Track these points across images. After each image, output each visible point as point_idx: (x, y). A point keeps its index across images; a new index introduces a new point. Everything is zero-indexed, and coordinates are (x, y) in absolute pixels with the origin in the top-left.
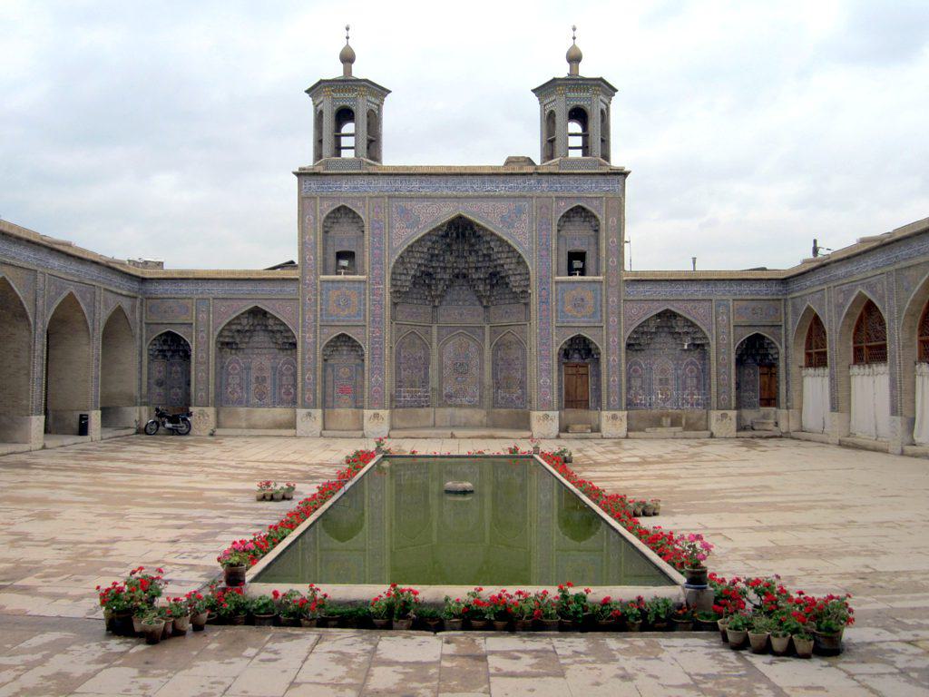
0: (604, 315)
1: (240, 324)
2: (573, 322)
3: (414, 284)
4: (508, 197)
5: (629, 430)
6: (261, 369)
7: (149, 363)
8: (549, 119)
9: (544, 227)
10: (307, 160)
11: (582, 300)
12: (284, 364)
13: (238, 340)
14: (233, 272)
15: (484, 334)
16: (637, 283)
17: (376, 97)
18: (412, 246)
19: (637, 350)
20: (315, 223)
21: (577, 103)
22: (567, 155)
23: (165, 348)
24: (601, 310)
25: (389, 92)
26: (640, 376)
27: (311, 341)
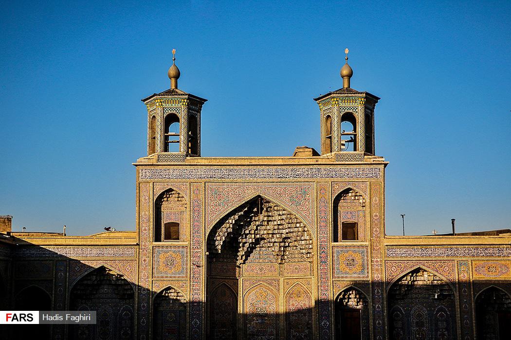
0: (370, 272)
1: (90, 280)
12: (124, 310)
17: (196, 106)
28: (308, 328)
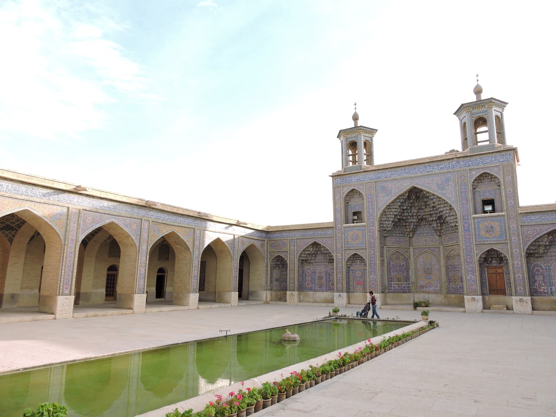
2: (487, 241)
3: (394, 225)
4: (440, 173)
5: (533, 309)
6: (320, 273)
7: (271, 270)
8: (464, 127)
9: (463, 187)
11: (492, 227)
13: (309, 259)
14: (304, 225)
16: (529, 214)
17: (369, 133)
19: (537, 257)
21: (479, 114)
23: (279, 263)
24: (506, 233)
25: (377, 130)
26: (542, 274)
27: (340, 258)
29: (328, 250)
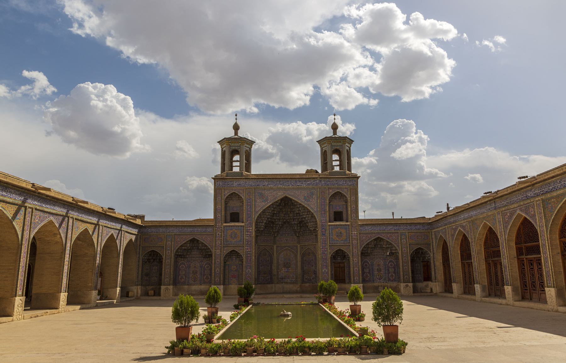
3: (266, 227)
6: (195, 267)
10: (218, 171)
11: (341, 233)
15: (297, 248)
18: (265, 210)
20: (222, 200)
22: (333, 169)
27: (218, 253)
28: (314, 274)
29: (206, 246)
